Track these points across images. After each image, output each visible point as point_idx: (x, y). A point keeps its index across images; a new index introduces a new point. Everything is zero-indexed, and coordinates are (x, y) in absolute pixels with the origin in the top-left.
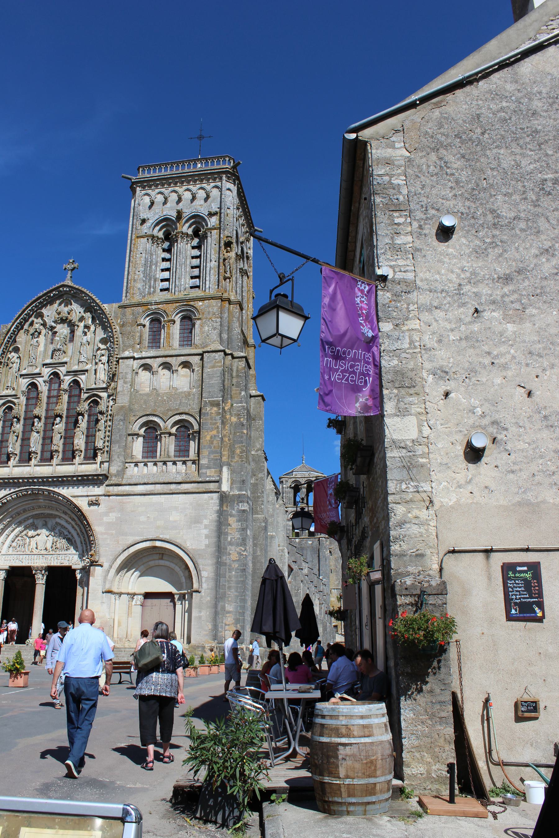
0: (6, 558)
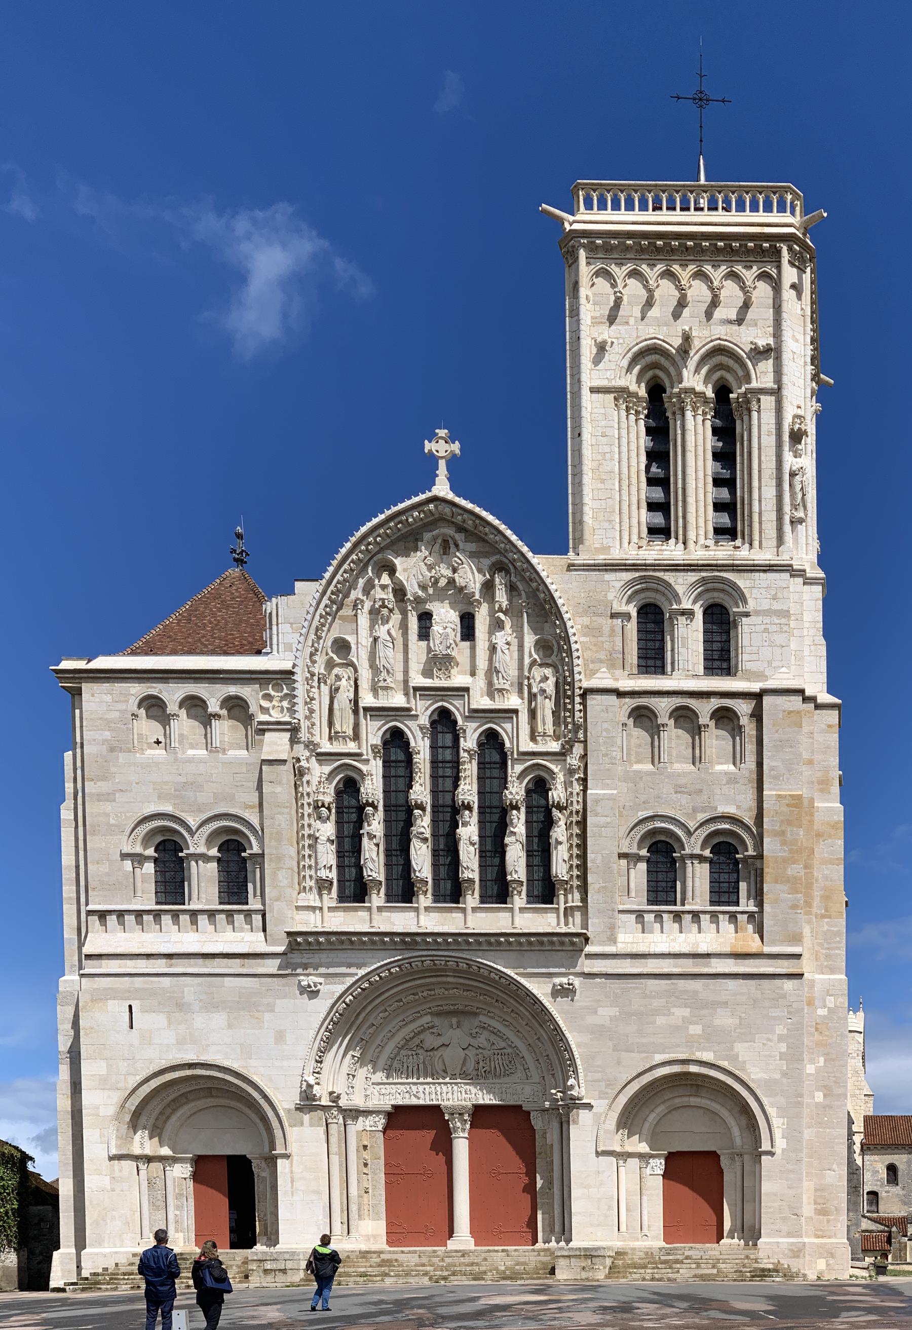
0: (383, 1091)
